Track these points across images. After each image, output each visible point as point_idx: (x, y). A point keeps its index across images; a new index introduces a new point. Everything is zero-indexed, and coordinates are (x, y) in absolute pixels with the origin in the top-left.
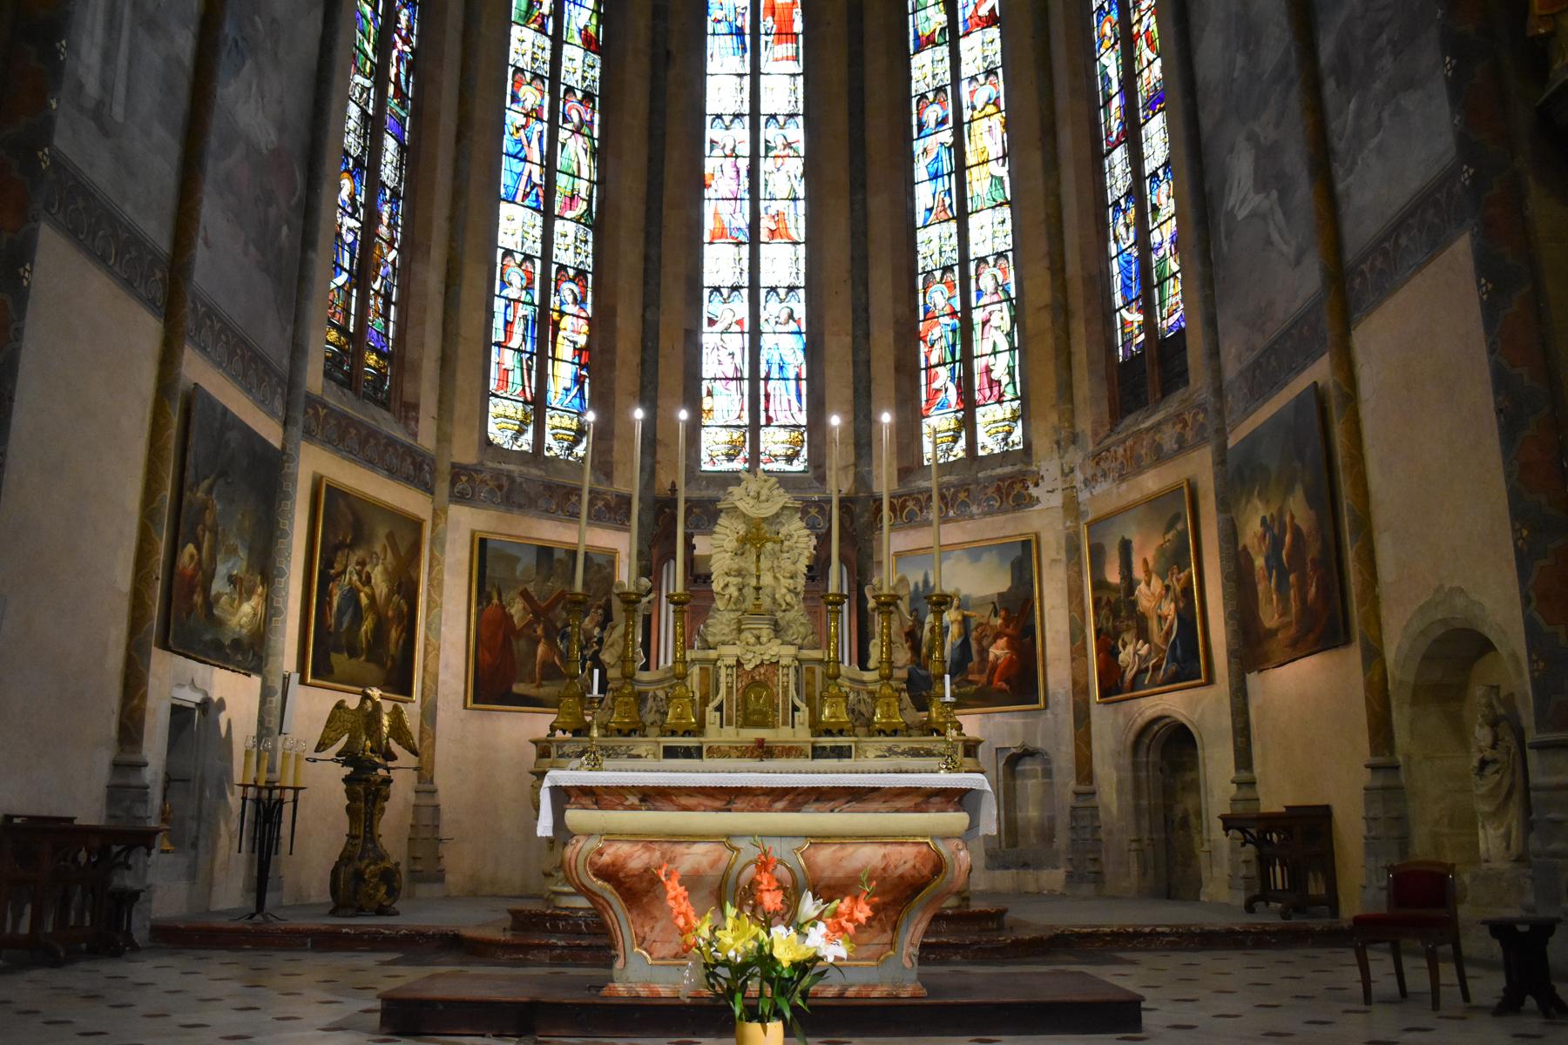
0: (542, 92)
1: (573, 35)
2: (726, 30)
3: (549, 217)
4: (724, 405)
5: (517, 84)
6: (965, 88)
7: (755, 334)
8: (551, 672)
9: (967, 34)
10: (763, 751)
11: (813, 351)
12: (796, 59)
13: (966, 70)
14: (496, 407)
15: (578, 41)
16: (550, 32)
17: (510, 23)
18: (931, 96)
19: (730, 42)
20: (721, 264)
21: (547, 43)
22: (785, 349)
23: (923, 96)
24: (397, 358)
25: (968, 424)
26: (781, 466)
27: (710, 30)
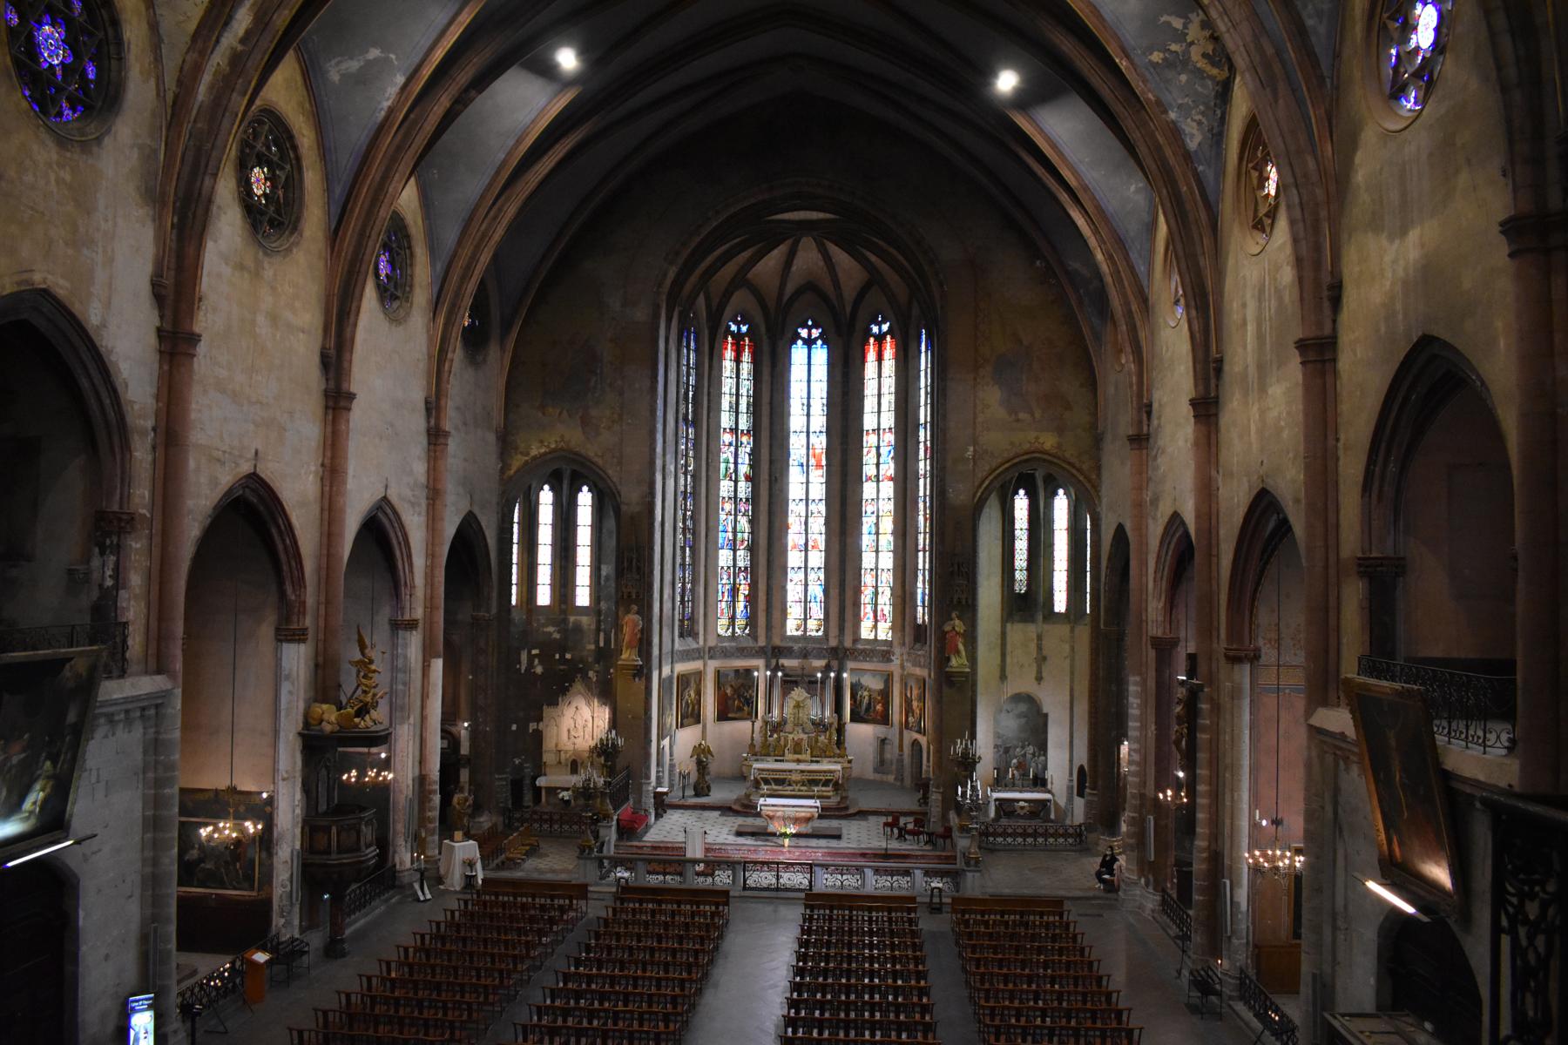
3: (735, 551)
4: (794, 612)
7: (806, 585)
8: (740, 709)
10: (799, 761)
11: (826, 592)
14: (720, 622)
20: (794, 559)
22: (817, 591)
24: (692, 619)
25: (875, 627)
26: (814, 634)
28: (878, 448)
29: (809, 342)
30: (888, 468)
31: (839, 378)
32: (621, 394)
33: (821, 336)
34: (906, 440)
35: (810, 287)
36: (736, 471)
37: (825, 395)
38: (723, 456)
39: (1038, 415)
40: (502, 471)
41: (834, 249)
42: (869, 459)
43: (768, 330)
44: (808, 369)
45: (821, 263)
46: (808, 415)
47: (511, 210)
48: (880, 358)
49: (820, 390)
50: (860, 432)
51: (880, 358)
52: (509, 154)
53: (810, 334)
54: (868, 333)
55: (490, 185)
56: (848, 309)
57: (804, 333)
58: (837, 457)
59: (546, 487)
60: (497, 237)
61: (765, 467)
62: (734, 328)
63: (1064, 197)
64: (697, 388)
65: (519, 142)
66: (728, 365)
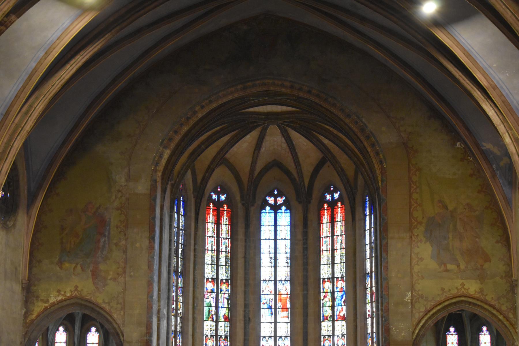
0: (213, 340)
1: (221, 319)
2: (267, 307)
5: (206, 340)
6: (336, 338)
9: (337, 321)
12: (288, 317)
13: (337, 332)
15: (223, 320)
16: (215, 320)
17: (203, 321)
18: (327, 337)
19: (268, 311)
21: (214, 324)
23: (324, 337)
27: (262, 307)
28: (333, 293)
29: (275, 208)
30: (341, 310)
31: (300, 236)
32: (125, 252)
33: (285, 203)
34: (355, 287)
35: (276, 164)
36: (217, 313)
37: (288, 250)
38: (206, 301)
39: (462, 267)
40: (26, 315)
41: (294, 135)
42: (326, 301)
43: (242, 197)
44: (275, 229)
45: (285, 145)
46: (275, 267)
47: (40, 107)
48: (333, 221)
49: (284, 246)
50: (318, 280)
51: (333, 221)
52: (40, 63)
53: (276, 201)
54: (323, 200)
55: (24, 87)
56: (307, 181)
57: (271, 200)
58: (300, 301)
59: (61, 329)
60: (28, 128)
61: (240, 310)
62: (214, 197)
63: (477, 94)
64: (185, 245)
65: (47, 53)
66: (210, 228)
